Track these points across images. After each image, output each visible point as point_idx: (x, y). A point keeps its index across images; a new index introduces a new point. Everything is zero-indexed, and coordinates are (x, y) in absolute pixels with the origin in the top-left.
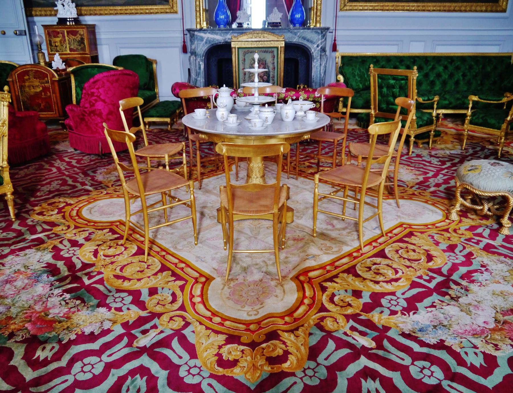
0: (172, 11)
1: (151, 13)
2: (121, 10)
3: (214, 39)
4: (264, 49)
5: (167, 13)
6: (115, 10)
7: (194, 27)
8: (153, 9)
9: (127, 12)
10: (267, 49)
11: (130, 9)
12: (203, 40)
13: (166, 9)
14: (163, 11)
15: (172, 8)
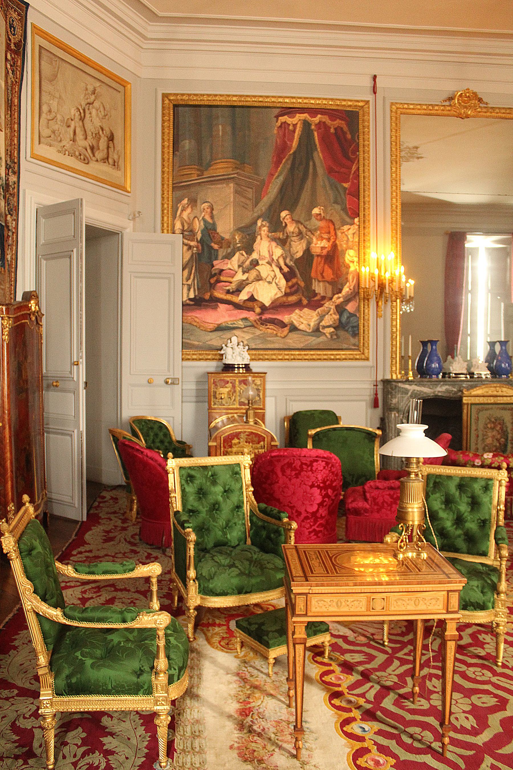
0: (363, 357)
1: (337, 359)
2: (298, 355)
3: (421, 391)
4: (502, 406)
5: (356, 359)
6: (292, 354)
7: (388, 377)
8: (339, 354)
9: (307, 357)
10: (506, 406)
11: (311, 355)
12: (408, 394)
13: (356, 354)
14: (352, 357)
15: (363, 354)
